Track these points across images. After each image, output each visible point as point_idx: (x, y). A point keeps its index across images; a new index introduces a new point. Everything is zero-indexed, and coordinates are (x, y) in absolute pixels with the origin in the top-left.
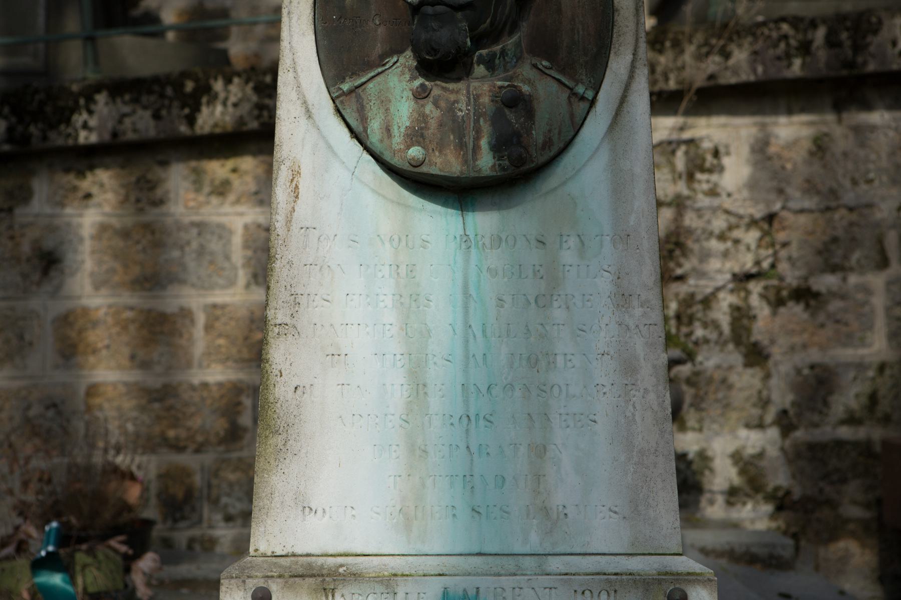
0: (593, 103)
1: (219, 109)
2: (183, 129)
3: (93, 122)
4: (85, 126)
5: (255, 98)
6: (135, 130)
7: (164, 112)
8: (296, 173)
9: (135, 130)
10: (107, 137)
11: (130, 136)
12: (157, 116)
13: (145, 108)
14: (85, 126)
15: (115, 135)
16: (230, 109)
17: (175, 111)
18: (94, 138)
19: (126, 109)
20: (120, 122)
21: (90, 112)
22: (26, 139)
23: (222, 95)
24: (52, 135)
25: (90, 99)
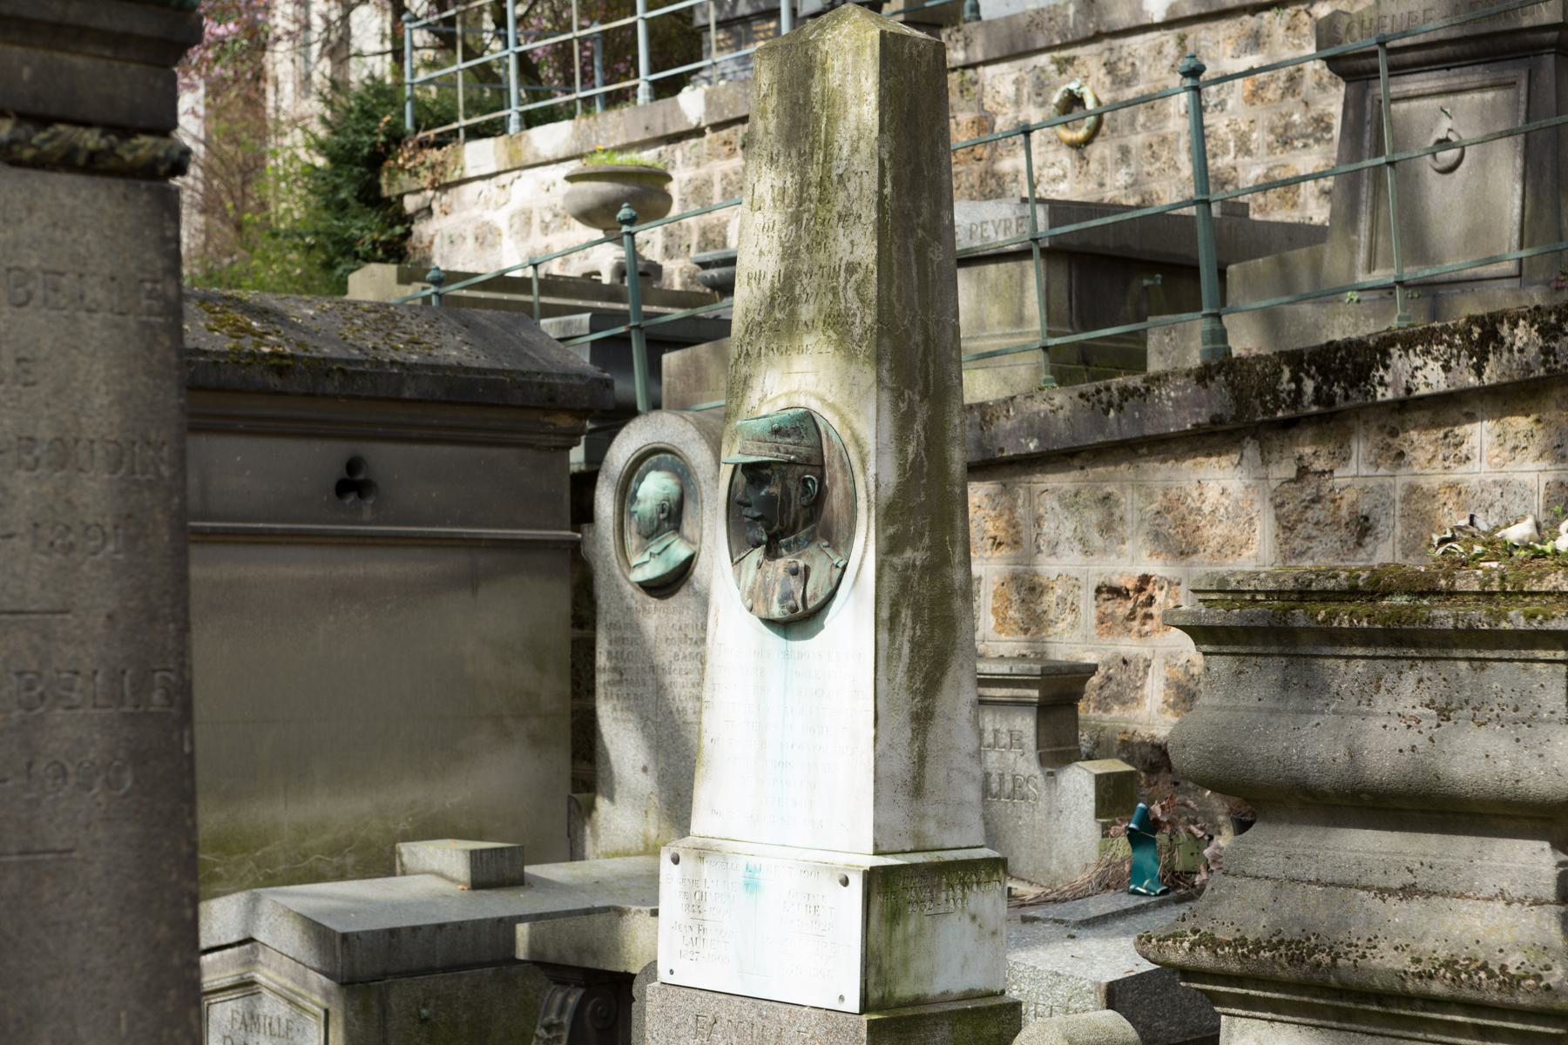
0: (844, 568)
1: (1506, 355)
2: (1472, 380)
3: (1388, 379)
4: (1382, 383)
5: (1540, 342)
6: (1427, 385)
7: (1453, 363)
8: (717, 610)
9: (1427, 385)
10: (1402, 393)
11: (1423, 391)
12: (1446, 368)
13: (1436, 359)
14: (1382, 383)
15: (1409, 390)
16: (1516, 355)
17: (1463, 361)
18: (1390, 395)
19: (1418, 362)
20: (1413, 376)
21: (1386, 367)
22: (1331, 401)
23: (1508, 340)
24: (1353, 393)
25: (1386, 354)
